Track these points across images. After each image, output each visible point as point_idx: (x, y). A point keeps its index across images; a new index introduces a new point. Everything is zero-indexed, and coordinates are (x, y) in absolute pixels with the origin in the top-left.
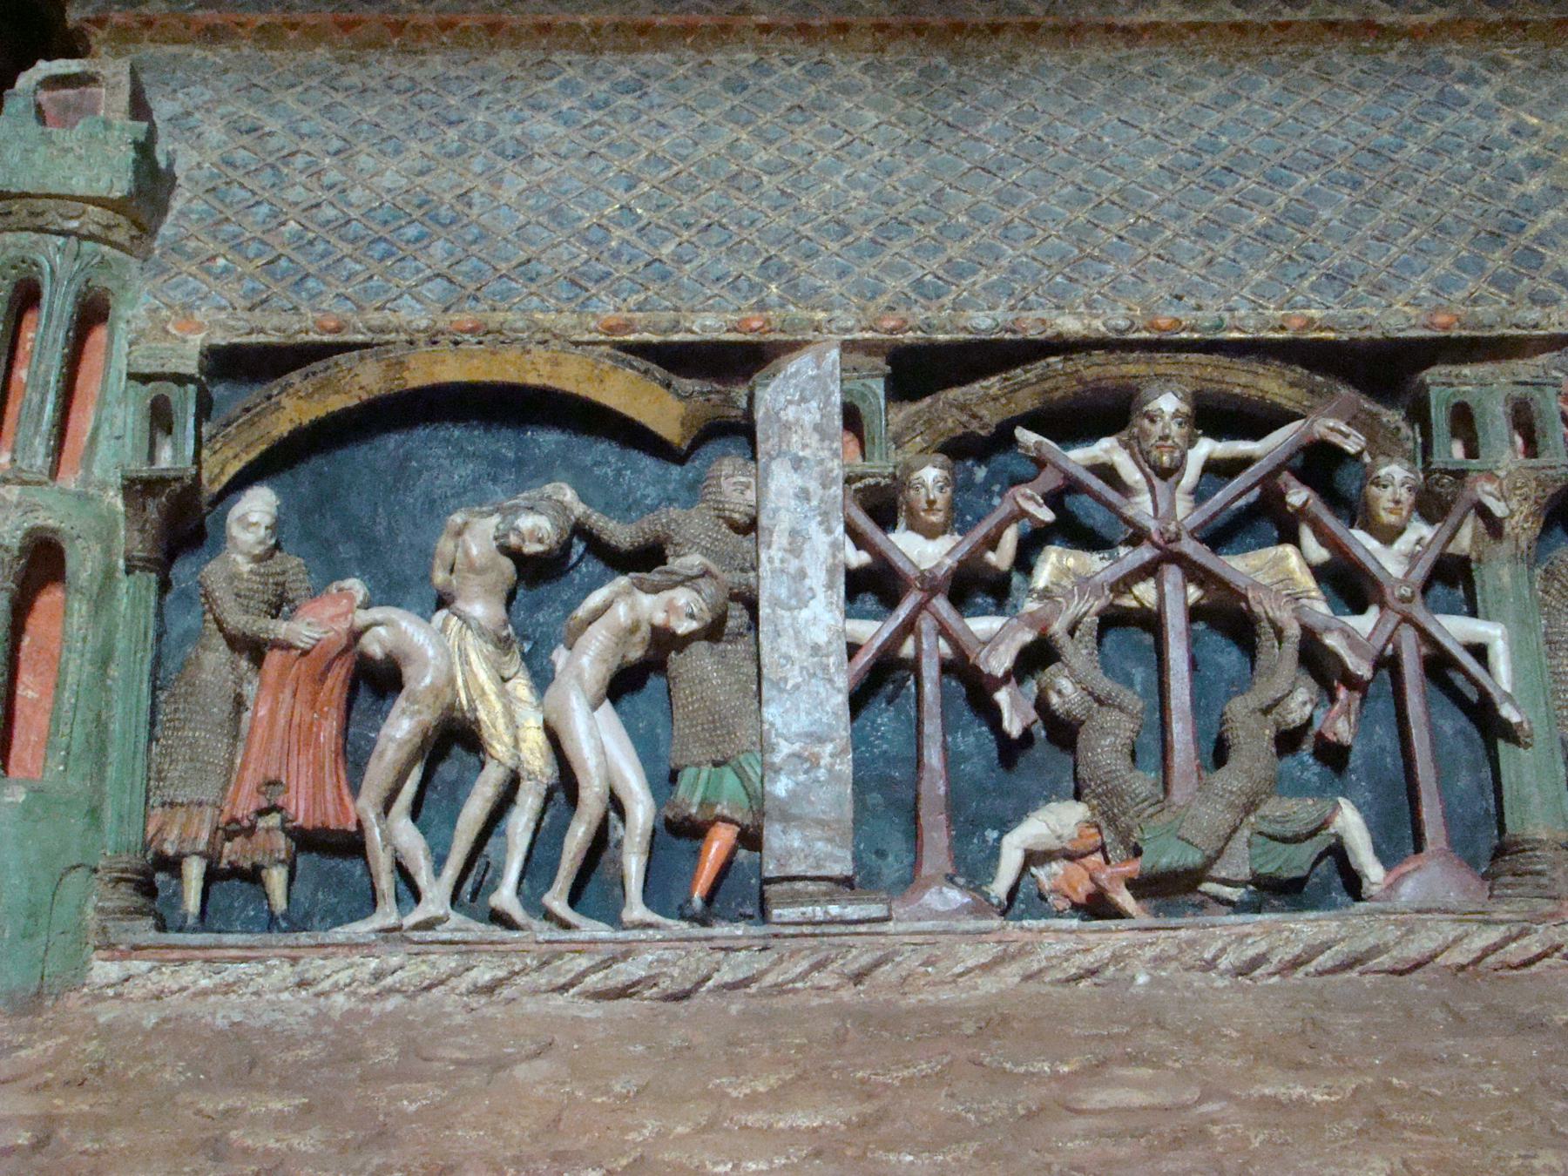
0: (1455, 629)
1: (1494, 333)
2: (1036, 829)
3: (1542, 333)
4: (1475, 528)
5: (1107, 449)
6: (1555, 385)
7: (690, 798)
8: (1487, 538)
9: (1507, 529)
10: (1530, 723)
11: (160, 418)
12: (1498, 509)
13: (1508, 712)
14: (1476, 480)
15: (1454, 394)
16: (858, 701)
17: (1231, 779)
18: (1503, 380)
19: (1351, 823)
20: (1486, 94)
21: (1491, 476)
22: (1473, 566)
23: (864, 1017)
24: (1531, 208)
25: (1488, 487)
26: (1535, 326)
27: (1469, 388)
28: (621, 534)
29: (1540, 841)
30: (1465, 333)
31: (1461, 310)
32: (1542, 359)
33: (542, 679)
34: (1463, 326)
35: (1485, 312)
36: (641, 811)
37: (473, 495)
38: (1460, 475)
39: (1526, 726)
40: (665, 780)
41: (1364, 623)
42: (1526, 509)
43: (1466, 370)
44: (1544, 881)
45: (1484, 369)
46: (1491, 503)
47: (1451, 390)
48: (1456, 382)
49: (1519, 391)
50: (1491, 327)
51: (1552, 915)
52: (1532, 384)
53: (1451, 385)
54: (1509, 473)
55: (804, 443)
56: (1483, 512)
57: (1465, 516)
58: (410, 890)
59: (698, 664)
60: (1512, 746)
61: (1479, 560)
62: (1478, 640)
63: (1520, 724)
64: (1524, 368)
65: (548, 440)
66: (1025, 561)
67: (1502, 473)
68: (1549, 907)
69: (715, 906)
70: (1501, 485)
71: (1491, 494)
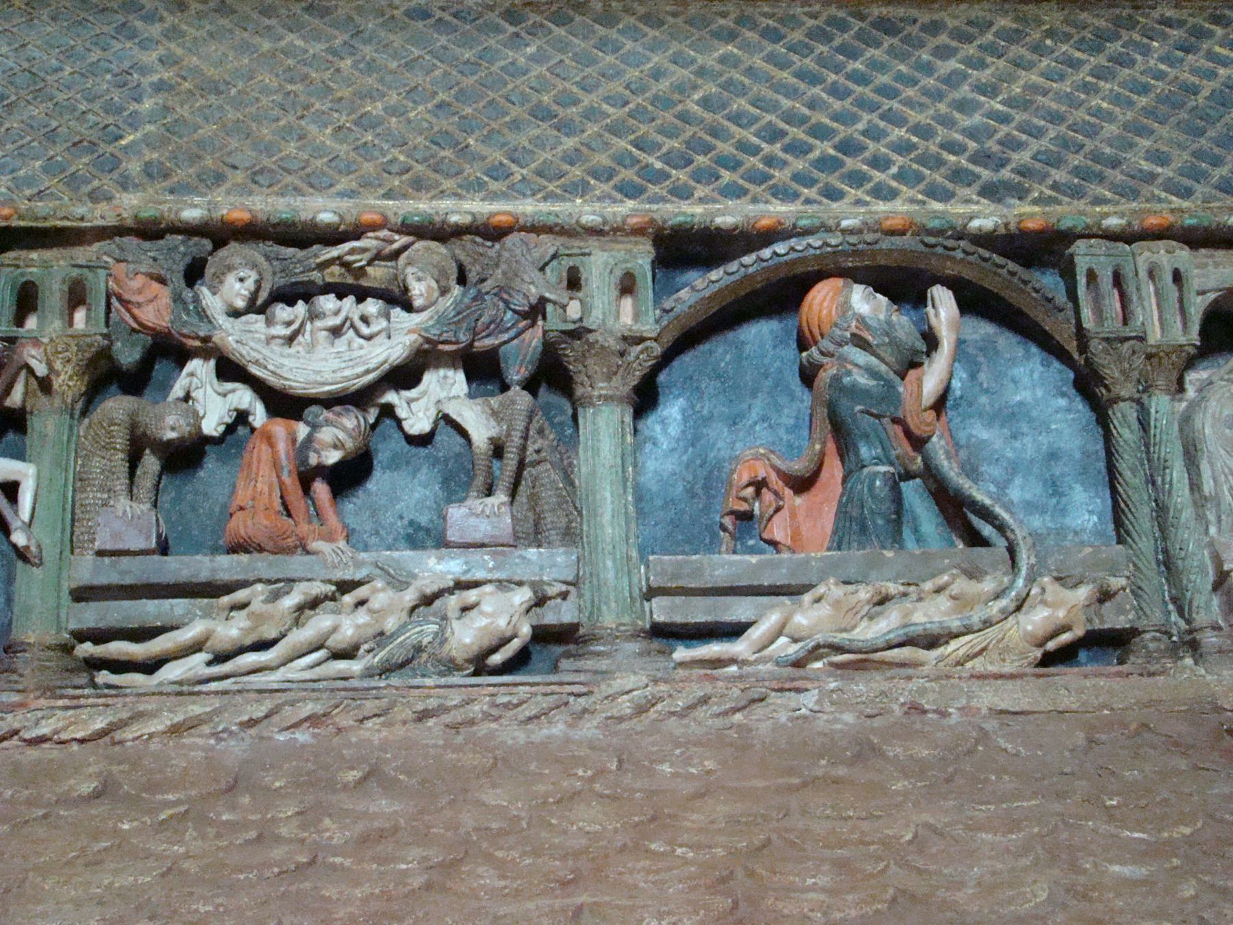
1: (47, 224)
3: (89, 224)
4: (27, 385)
6: (105, 268)
8: (39, 394)
9: (56, 386)
10: (39, 546)
12: (41, 370)
13: (19, 538)
14: (24, 346)
15: (22, 275)
18: (62, 263)
20: (155, 30)
21: (36, 342)
22: (28, 416)
24: (134, 122)
25: (33, 352)
26: (82, 219)
27: (34, 270)
29: (29, 644)
30: (22, 223)
31: (23, 206)
32: (96, 246)
34: (21, 217)
35: (41, 207)
38: (12, 340)
39: (33, 549)
42: (70, 369)
43: (34, 255)
44: (15, 677)
45: (48, 254)
46: (34, 363)
47: (19, 271)
48: (22, 264)
49: (75, 272)
50: (45, 219)
51: (22, 705)
52: (88, 267)
53: (18, 266)
54: (51, 340)
56: (31, 371)
57: (17, 374)
60: (29, 566)
61: (31, 413)
62: (13, 478)
63: (27, 547)
64: (84, 254)
67: (46, 340)
68: (15, 698)
70: (45, 350)
71: (33, 357)
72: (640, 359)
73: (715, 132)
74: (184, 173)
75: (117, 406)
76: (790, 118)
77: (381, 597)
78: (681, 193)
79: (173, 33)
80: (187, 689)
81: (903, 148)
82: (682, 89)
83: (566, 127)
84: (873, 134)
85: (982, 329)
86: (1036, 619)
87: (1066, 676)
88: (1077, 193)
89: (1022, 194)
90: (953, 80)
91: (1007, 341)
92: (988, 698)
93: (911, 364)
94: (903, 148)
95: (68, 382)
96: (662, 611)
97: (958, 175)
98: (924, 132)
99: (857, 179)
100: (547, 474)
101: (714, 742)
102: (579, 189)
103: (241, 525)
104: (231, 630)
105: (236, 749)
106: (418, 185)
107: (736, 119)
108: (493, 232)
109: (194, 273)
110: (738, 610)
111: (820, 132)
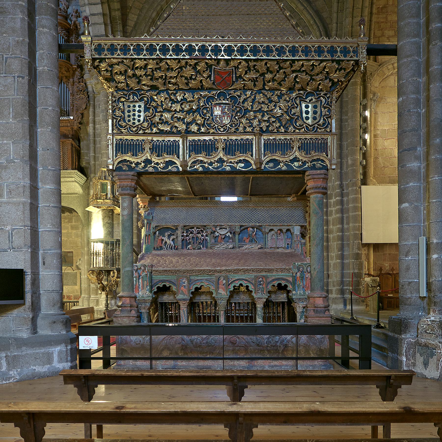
0: (207, 238)
2: (189, 246)
5: (193, 229)
7: (175, 245)
11: (154, 229)
16: (182, 241)
17: (197, 244)
19: (201, 246)
20: (213, 210)
23: (181, 254)
28: (172, 233)
33: (169, 240)
36: (173, 245)
37: (166, 232)
40: (174, 245)
41: (203, 237)
55: (180, 230)
58: (164, 249)
59: (176, 240)
65: (169, 229)
66: (189, 234)
69: (176, 249)
72: (239, 232)
73: (244, 218)
74: (215, 222)
75: (212, 235)
76: (249, 217)
77: (225, 245)
78: (242, 223)
79: (214, 211)
80: (216, 249)
81: (254, 219)
82: (243, 214)
83: (236, 218)
84: (253, 218)
85: (258, 230)
86: (258, 247)
87: (259, 249)
88: (263, 223)
89: (260, 223)
90: (258, 214)
91: (259, 231)
92: (255, 251)
93: (253, 232)
94: (254, 219)
95: (210, 233)
96: (239, 246)
97: (257, 221)
98: (256, 218)
99: (251, 222)
100: (234, 238)
101: (241, 253)
102: (236, 223)
103: (218, 241)
104: (218, 247)
105: (219, 252)
106: (228, 222)
107: (246, 217)
108: (231, 225)
109: (216, 227)
110: (243, 246)
111: (250, 218)
